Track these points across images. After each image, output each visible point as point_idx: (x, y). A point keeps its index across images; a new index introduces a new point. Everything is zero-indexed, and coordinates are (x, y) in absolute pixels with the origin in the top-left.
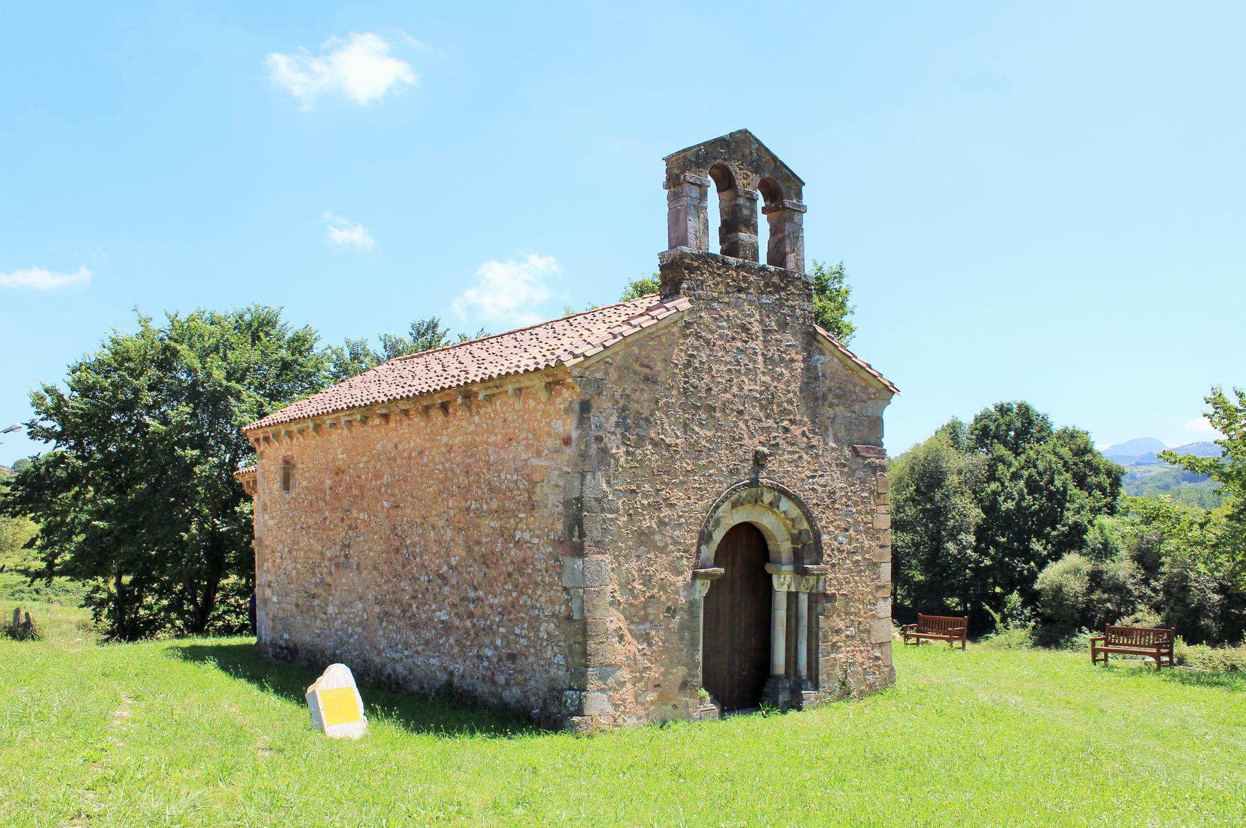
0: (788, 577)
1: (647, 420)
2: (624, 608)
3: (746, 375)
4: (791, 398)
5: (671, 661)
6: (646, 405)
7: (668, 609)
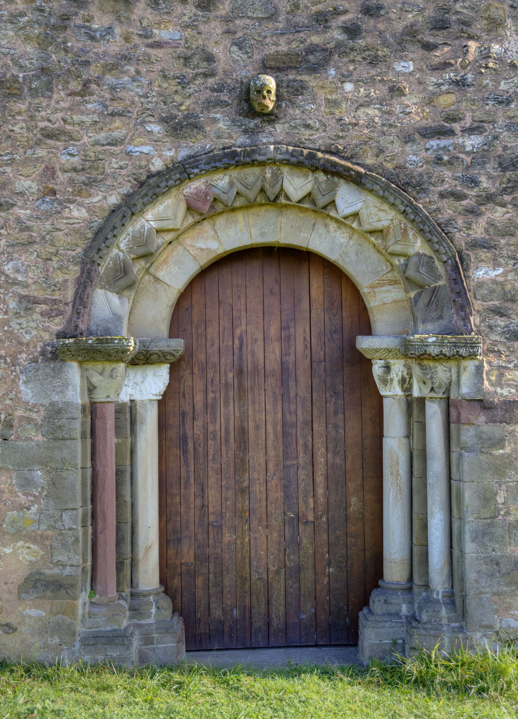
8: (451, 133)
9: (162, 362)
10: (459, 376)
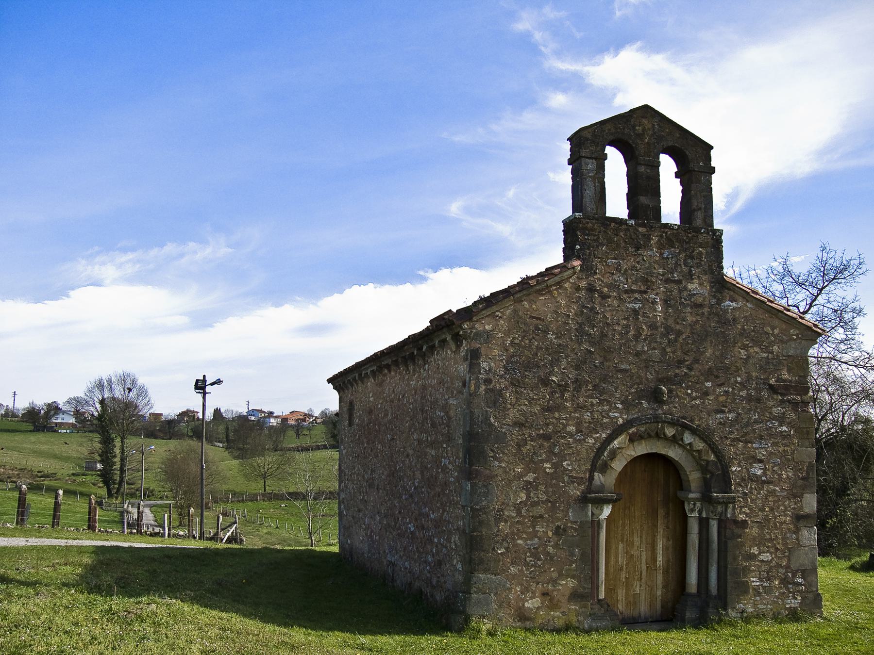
0: (698, 504)
8: (723, 412)
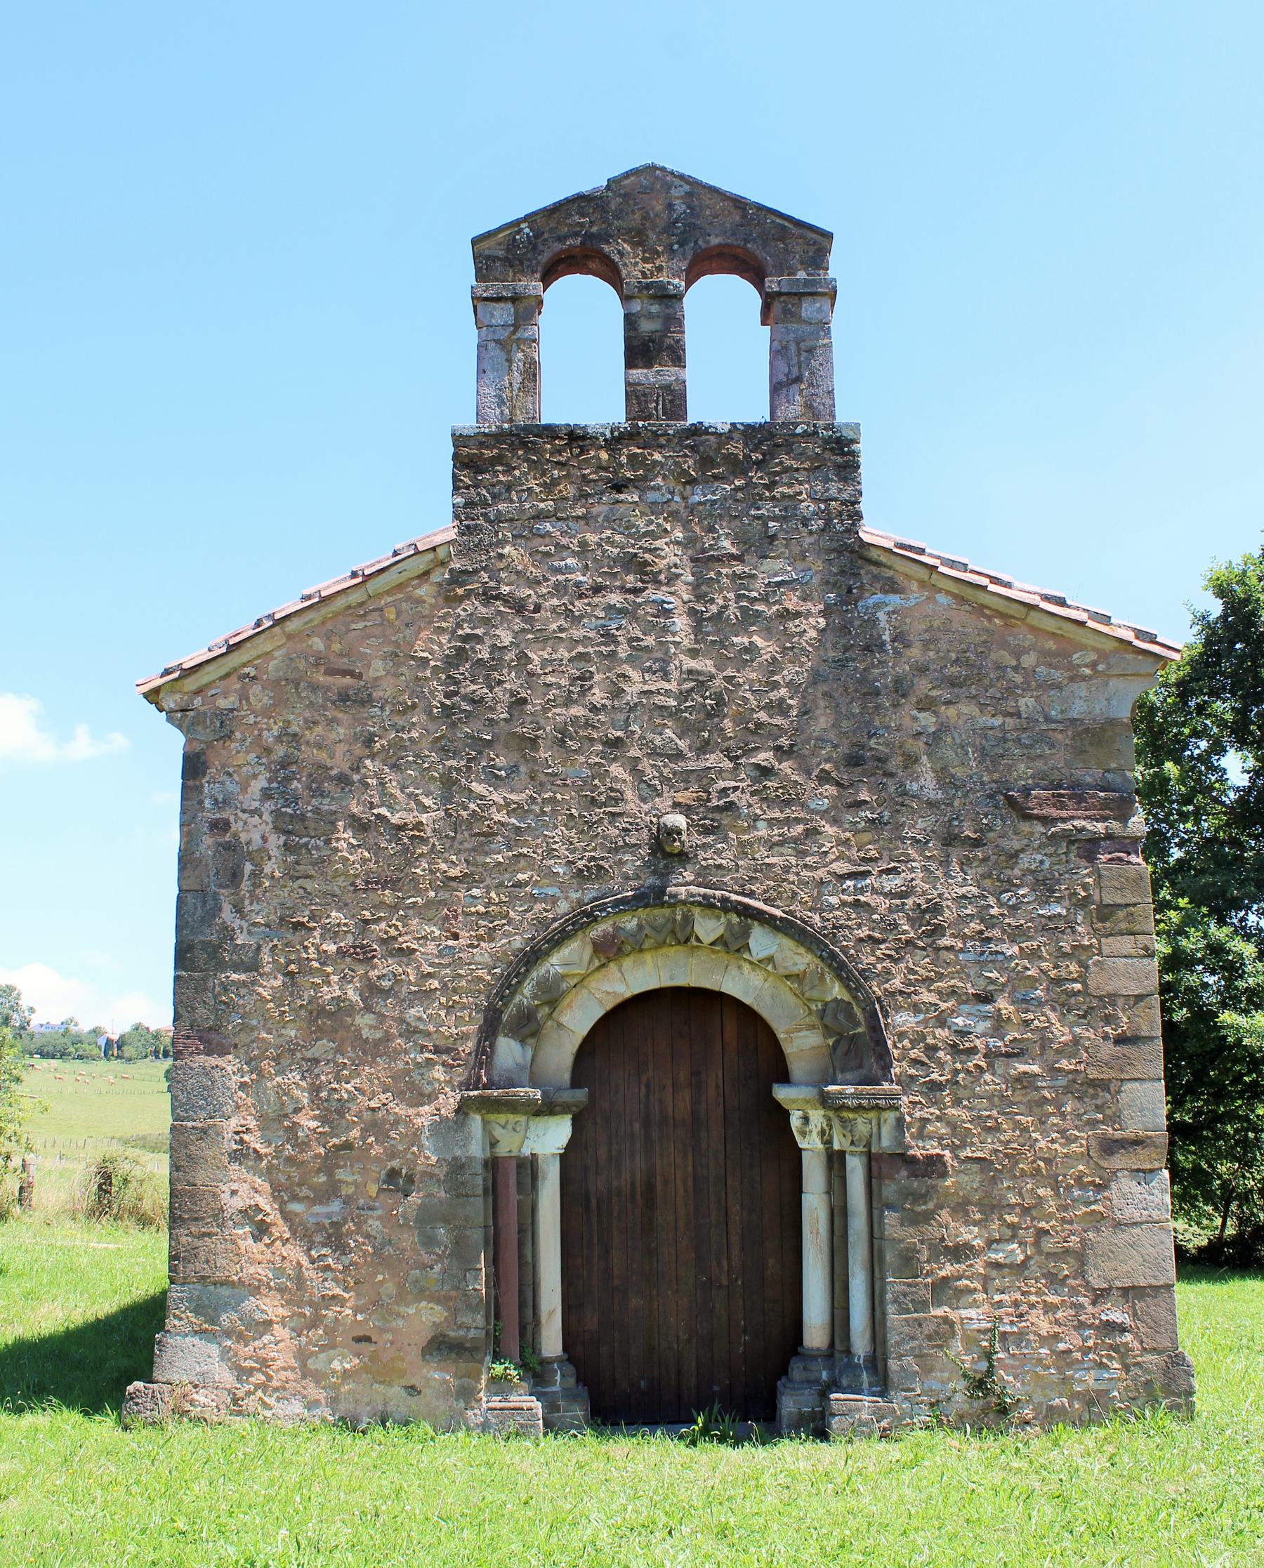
1: (343, 780)
2: (270, 1168)
3: (630, 660)
4: (782, 700)
5: (400, 1287)
6: (341, 748)
7: (393, 1175)
9: (563, 1112)
10: (879, 1128)
